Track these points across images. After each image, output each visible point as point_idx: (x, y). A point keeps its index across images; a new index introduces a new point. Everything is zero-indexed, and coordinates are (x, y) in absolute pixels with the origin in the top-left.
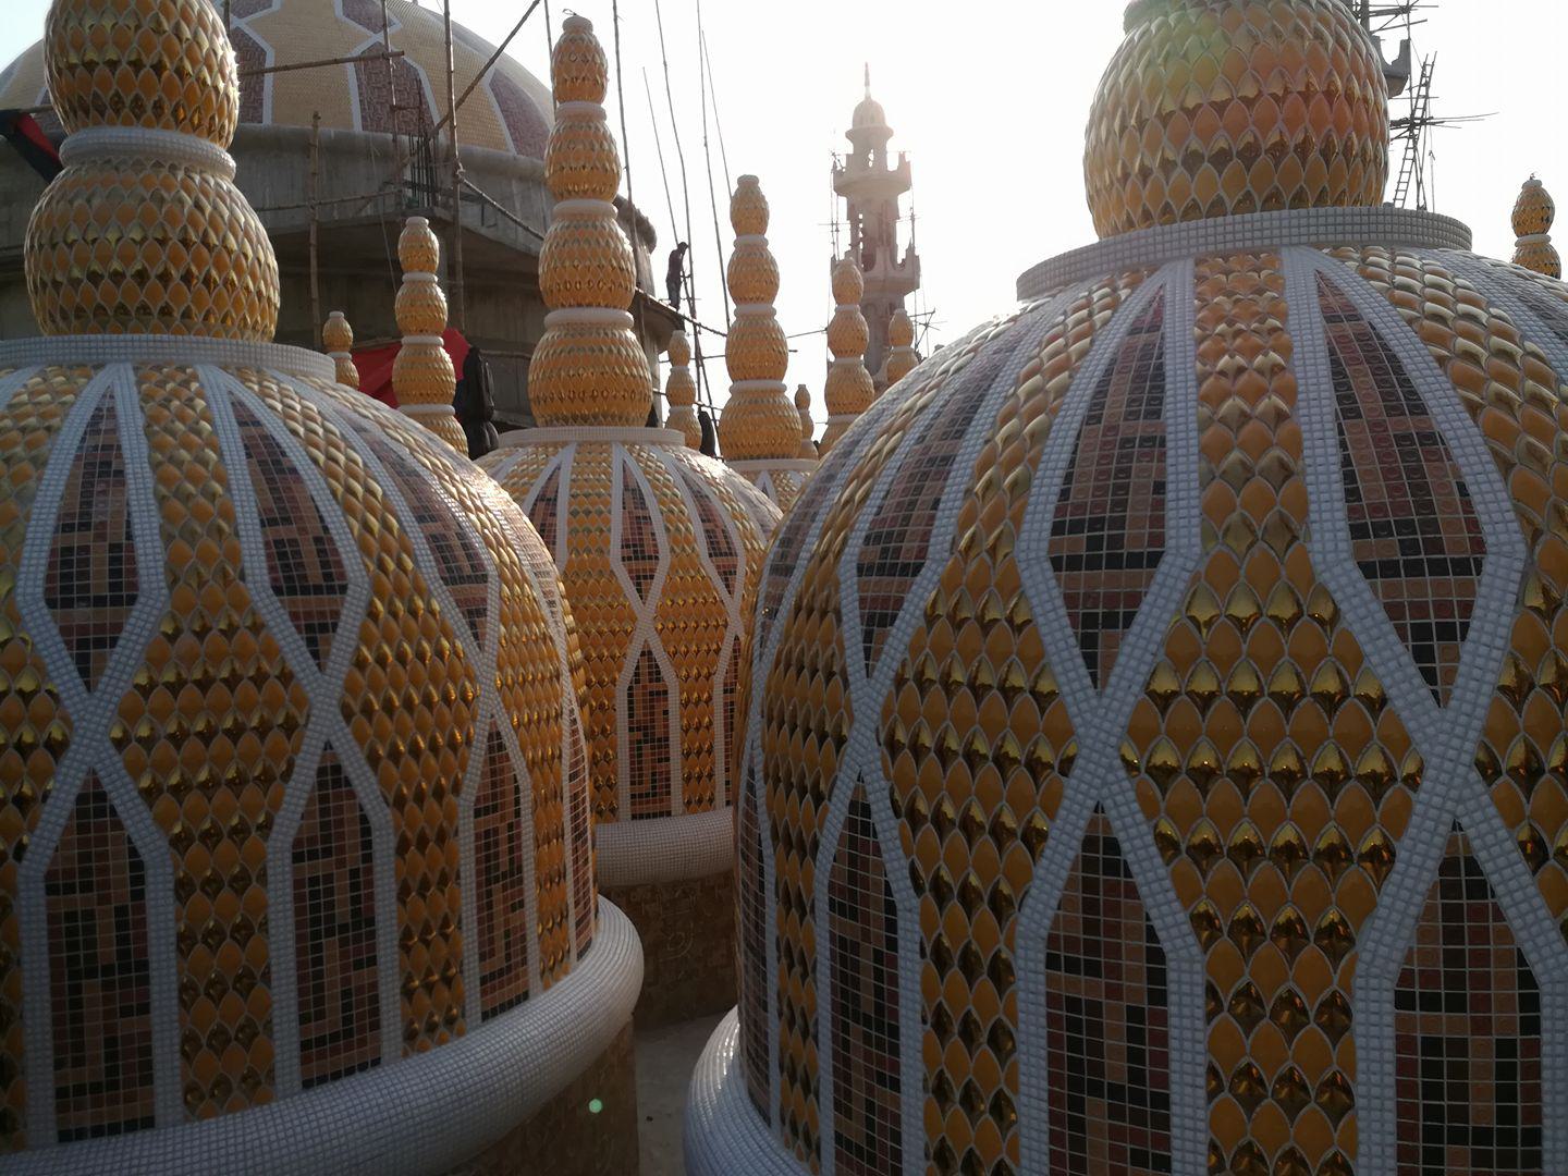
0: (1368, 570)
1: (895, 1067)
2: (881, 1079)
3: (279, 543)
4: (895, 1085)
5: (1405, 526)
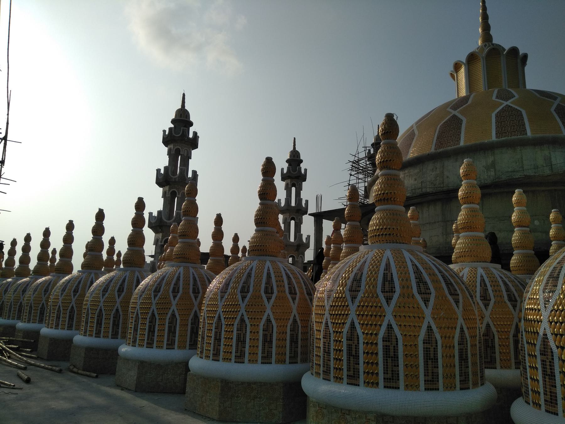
2: (552, 386)
4: (555, 387)
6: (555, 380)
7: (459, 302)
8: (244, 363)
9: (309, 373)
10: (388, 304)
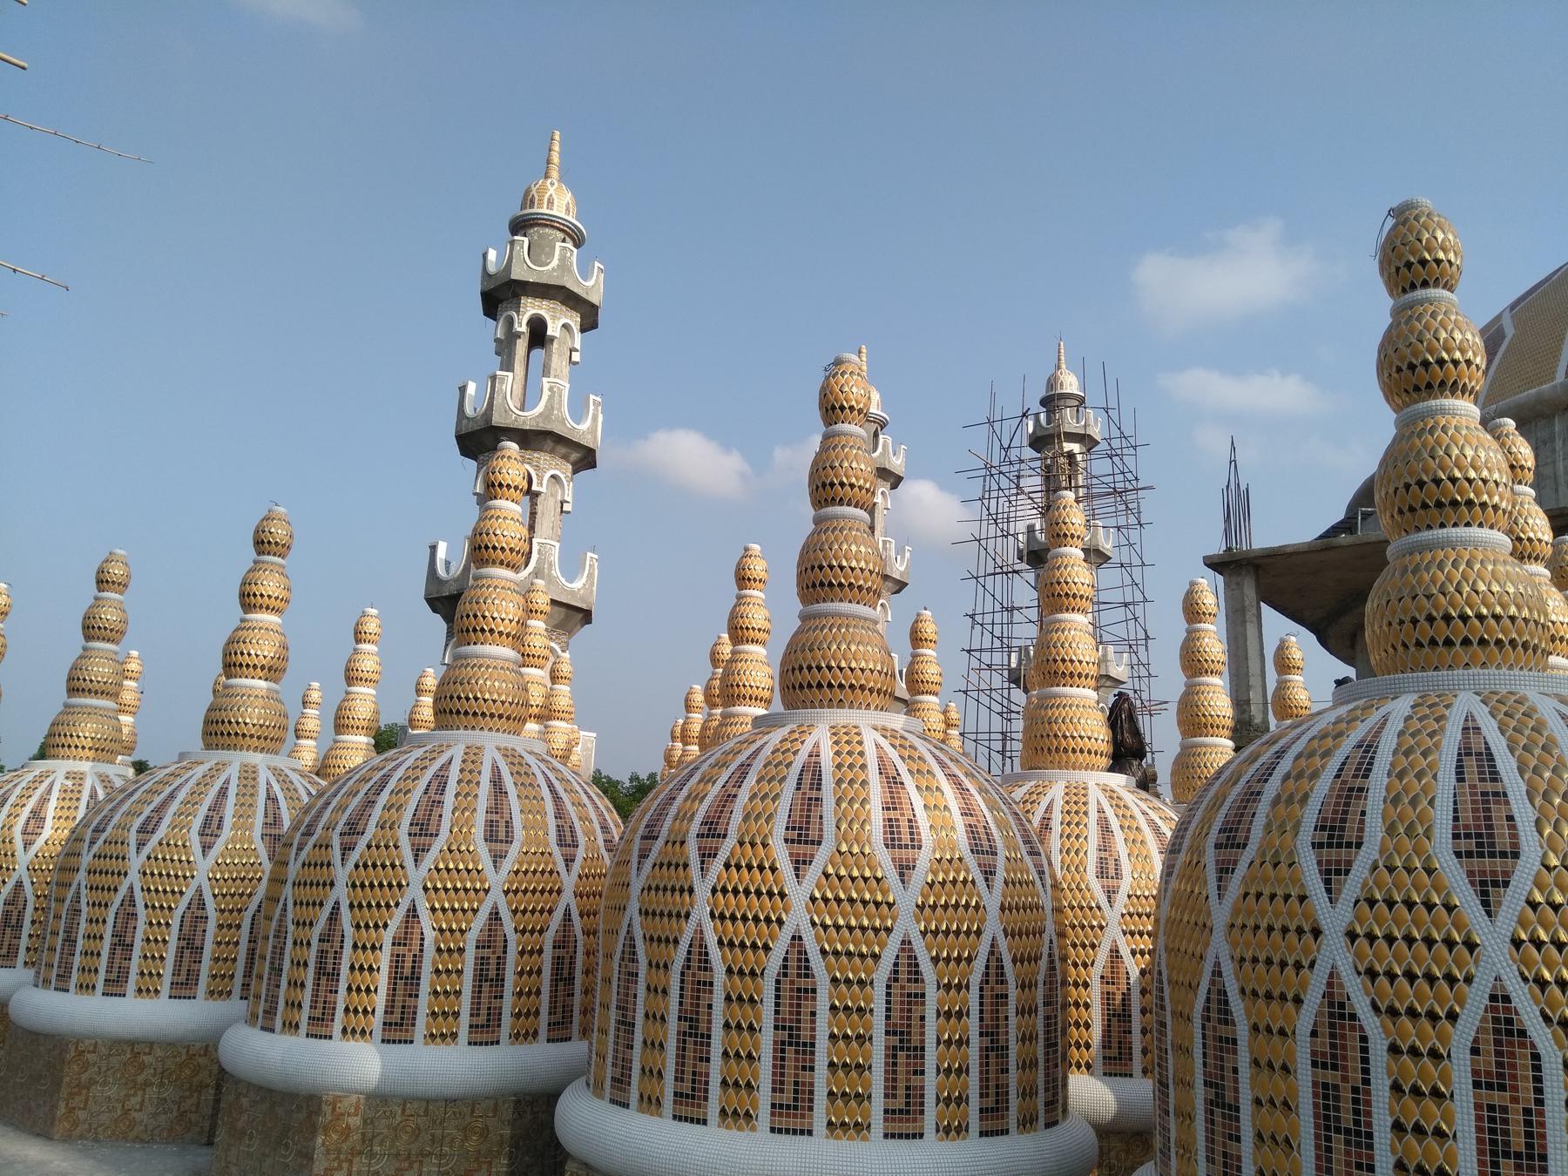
0: (1458, 855)
1: (1238, 1129)
3: (890, 820)
4: (1238, 1139)
5: (1479, 836)
6: (1237, 1119)
7: (993, 873)
9: (581, 1082)
10: (495, 867)
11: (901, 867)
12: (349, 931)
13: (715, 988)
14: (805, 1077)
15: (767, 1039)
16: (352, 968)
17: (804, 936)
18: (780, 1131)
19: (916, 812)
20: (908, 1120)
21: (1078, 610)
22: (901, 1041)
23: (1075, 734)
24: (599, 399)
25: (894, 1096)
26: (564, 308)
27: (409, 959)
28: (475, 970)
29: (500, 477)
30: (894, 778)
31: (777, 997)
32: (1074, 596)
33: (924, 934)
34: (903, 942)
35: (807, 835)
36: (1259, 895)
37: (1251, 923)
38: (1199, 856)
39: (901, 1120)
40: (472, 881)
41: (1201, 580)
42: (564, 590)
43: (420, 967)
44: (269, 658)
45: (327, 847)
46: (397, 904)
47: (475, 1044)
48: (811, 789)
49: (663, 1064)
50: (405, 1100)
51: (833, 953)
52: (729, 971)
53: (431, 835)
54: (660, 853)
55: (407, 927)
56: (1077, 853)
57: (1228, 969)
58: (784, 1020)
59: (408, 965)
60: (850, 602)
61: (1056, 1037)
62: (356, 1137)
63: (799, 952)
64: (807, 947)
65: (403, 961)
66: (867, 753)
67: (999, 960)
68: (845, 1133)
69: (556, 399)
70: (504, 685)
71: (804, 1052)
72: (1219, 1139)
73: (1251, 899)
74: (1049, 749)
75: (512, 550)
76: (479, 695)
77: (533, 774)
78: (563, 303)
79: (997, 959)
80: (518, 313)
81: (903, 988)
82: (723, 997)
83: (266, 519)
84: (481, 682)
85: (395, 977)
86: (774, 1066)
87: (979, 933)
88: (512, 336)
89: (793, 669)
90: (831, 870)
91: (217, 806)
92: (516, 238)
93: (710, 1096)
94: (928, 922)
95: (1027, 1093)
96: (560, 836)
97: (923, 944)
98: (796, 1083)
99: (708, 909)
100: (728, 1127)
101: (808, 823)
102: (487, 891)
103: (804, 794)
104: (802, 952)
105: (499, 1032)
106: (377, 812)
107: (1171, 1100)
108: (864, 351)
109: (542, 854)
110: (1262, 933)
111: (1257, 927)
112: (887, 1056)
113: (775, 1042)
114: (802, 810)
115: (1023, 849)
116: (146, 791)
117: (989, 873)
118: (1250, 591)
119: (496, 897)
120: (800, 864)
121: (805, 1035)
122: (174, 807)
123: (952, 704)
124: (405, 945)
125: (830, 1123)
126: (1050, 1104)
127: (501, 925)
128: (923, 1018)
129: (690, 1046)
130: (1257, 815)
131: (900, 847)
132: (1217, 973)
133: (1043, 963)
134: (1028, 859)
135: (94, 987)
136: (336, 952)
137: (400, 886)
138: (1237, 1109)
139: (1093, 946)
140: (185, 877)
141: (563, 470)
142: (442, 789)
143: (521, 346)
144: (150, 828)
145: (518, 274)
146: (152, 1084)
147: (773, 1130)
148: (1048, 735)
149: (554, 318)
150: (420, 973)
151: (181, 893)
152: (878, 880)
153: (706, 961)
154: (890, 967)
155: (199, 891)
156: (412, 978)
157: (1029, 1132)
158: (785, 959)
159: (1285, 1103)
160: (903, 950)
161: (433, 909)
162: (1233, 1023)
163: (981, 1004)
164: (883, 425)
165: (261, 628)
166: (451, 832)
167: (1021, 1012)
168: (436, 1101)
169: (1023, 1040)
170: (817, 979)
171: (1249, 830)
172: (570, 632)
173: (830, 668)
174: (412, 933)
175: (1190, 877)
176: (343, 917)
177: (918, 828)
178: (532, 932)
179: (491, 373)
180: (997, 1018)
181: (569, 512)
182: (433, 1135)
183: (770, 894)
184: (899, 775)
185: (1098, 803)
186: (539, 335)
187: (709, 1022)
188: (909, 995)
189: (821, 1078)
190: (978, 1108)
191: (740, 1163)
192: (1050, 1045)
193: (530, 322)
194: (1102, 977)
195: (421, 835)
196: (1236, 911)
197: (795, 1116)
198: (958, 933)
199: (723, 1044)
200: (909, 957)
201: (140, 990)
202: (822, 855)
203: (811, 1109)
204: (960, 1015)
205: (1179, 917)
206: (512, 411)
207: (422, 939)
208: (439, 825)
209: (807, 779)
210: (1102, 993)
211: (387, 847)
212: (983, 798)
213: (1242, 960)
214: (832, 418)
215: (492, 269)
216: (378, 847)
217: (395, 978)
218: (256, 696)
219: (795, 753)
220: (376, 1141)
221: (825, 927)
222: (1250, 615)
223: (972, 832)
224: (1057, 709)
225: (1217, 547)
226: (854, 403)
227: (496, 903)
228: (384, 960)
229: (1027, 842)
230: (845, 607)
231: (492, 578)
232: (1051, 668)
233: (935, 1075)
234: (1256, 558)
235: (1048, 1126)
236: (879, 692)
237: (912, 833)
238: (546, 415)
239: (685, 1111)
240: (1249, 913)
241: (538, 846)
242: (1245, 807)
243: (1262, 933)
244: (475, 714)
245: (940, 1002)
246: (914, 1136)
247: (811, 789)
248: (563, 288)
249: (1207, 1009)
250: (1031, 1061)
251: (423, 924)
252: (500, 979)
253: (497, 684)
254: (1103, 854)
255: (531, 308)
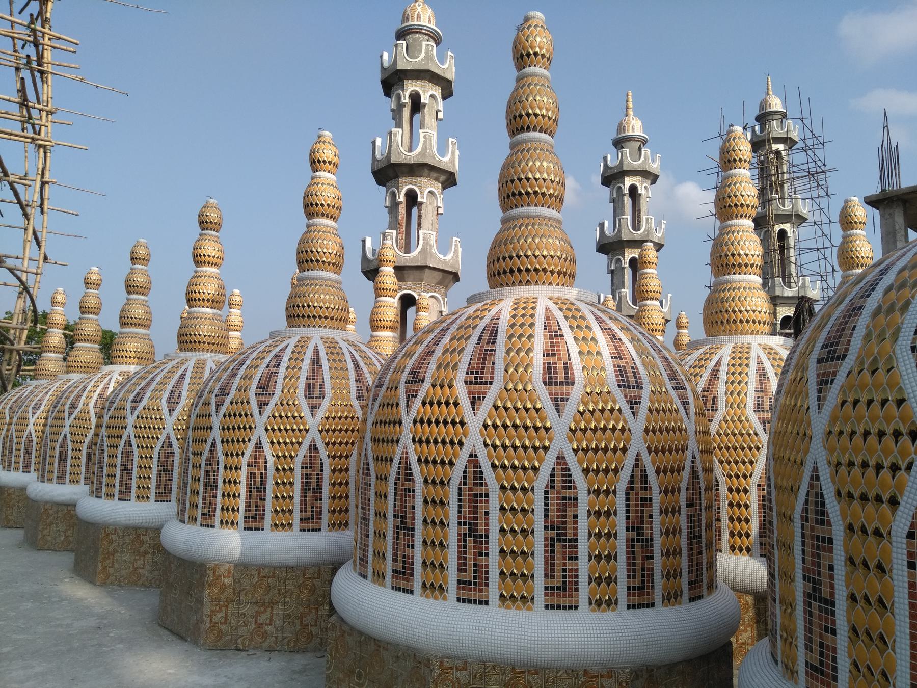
1: (834, 622)
2: (826, 629)
3: (549, 363)
4: (834, 632)
6: (833, 614)
8: (263, 529)
11: (556, 399)
12: (222, 458)
13: (416, 494)
14: (482, 560)
15: (453, 532)
16: (224, 481)
17: (478, 454)
18: (464, 601)
19: (572, 357)
20: (565, 595)
21: (746, 216)
22: (558, 534)
23: (743, 309)
24: (455, 140)
25: (553, 577)
26: (430, 84)
27: (258, 475)
28: (302, 482)
29: (318, 156)
30: (556, 332)
31: (460, 500)
32: (742, 205)
33: (575, 451)
34: (558, 458)
35: (482, 378)
36: (856, 402)
37: (848, 429)
38: (803, 372)
39: (558, 595)
40: (297, 424)
41: (853, 198)
42: (440, 261)
43: (266, 481)
44: (211, 294)
45: (209, 404)
46: (249, 440)
47: (305, 530)
48: (488, 343)
49: (386, 549)
50: (260, 567)
51: (532, 468)
52: (426, 481)
53: (270, 394)
54: (383, 397)
55: (256, 455)
56: (739, 394)
57: (825, 473)
58: (465, 518)
59: (258, 479)
60: (536, 205)
61: (699, 531)
62: (229, 591)
63: (475, 467)
64: (482, 462)
65: (255, 477)
66: (537, 316)
67: (644, 471)
68: (514, 603)
69: (428, 142)
70: (332, 297)
71: (481, 542)
72: (816, 629)
73: (849, 406)
74: (722, 322)
75: (328, 205)
76: (311, 304)
77: (343, 353)
78: (430, 81)
79: (642, 471)
80: (403, 91)
81: (558, 493)
82: (422, 500)
83: (204, 207)
84: (311, 295)
85: (250, 487)
86: (459, 552)
87: (624, 450)
88: (401, 106)
89: (494, 261)
90: (499, 404)
91: (178, 385)
92: (398, 42)
93: (415, 573)
94: (579, 441)
95: (671, 574)
96: (359, 393)
97: (575, 459)
98: (475, 565)
99: (411, 436)
100: (427, 597)
101: (483, 368)
102: (307, 431)
103: (482, 347)
104: (477, 466)
105: (321, 523)
106: (237, 381)
107: (777, 589)
108: (630, 94)
109: (346, 405)
110: (858, 438)
111: (853, 433)
112: (546, 546)
113: (459, 535)
114: (479, 359)
115: (669, 385)
116: (139, 378)
117: (634, 404)
118: (899, 219)
119: (314, 434)
120: (476, 399)
121: (481, 529)
122: (153, 386)
123: (683, 313)
124: (255, 466)
125: (502, 596)
126: (694, 583)
127: (318, 452)
128: (576, 517)
129: (401, 536)
130: (857, 328)
131: (556, 384)
132: (815, 477)
133: (686, 474)
134: (673, 394)
135: (114, 495)
136: (215, 472)
137: (250, 428)
138: (833, 604)
139: (751, 463)
140: (159, 428)
141: (436, 187)
142: (278, 365)
143: (406, 112)
144: (138, 400)
145: (400, 66)
146: (148, 553)
147: (459, 600)
148: (721, 312)
149: (424, 91)
150: (265, 484)
151: (158, 438)
152: (537, 410)
153: (410, 474)
154: (548, 477)
155: (168, 436)
156: (261, 488)
157: (673, 605)
158: (465, 472)
159: (880, 601)
160: (558, 464)
161: (272, 443)
162: (829, 524)
163: (627, 506)
164: (644, 142)
165: (205, 276)
166: (283, 392)
167: (664, 511)
168: (280, 567)
169: (667, 533)
170: (489, 487)
171: (849, 342)
172: (447, 287)
173: (519, 257)
174: (259, 459)
175: (794, 392)
176: (218, 451)
177: (572, 369)
178: (340, 457)
179: (388, 131)
180: (642, 517)
181: (442, 214)
182: (279, 590)
183: (454, 423)
184: (560, 329)
185: (758, 357)
186: (416, 105)
187: (413, 519)
188: (564, 499)
189: (494, 562)
190: (626, 587)
191: (431, 625)
192: (694, 537)
193: (411, 96)
194: (759, 485)
195: (263, 395)
196: (834, 419)
197: (475, 590)
198: (605, 450)
199: (423, 536)
200: (564, 470)
201: (138, 497)
202: (493, 392)
203: (487, 585)
204: (608, 514)
205: (784, 429)
206: (404, 155)
207: (266, 463)
208: (274, 388)
209: (486, 336)
210: (759, 497)
211: (242, 403)
212: (634, 346)
213: (839, 464)
214: (521, 64)
215: (386, 65)
216: (237, 403)
217: (250, 488)
218: (206, 318)
219: (482, 318)
220: (243, 593)
221: (495, 447)
222: (900, 235)
223: (621, 371)
224: (728, 291)
225: (874, 189)
226: (537, 50)
227: (313, 438)
228: (243, 476)
229: (673, 378)
230: (532, 210)
231: (317, 225)
232: (723, 261)
233: (587, 560)
234: (904, 194)
235: (691, 600)
236: (559, 273)
237: (566, 373)
238: (423, 153)
239: (400, 583)
240: (846, 419)
241: (343, 400)
242: (846, 323)
243: (858, 438)
244: (309, 317)
245: (590, 504)
246: (570, 608)
247: (488, 343)
248: (429, 71)
249: (806, 510)
250: (675, 550)
251: (266, 452)
252: (319, 489)
253: (322, 296)
254: (760, 394)
255: (411, 87)
